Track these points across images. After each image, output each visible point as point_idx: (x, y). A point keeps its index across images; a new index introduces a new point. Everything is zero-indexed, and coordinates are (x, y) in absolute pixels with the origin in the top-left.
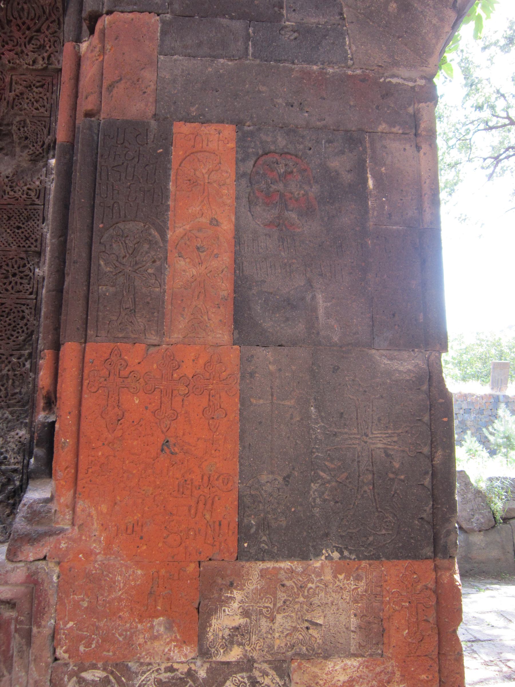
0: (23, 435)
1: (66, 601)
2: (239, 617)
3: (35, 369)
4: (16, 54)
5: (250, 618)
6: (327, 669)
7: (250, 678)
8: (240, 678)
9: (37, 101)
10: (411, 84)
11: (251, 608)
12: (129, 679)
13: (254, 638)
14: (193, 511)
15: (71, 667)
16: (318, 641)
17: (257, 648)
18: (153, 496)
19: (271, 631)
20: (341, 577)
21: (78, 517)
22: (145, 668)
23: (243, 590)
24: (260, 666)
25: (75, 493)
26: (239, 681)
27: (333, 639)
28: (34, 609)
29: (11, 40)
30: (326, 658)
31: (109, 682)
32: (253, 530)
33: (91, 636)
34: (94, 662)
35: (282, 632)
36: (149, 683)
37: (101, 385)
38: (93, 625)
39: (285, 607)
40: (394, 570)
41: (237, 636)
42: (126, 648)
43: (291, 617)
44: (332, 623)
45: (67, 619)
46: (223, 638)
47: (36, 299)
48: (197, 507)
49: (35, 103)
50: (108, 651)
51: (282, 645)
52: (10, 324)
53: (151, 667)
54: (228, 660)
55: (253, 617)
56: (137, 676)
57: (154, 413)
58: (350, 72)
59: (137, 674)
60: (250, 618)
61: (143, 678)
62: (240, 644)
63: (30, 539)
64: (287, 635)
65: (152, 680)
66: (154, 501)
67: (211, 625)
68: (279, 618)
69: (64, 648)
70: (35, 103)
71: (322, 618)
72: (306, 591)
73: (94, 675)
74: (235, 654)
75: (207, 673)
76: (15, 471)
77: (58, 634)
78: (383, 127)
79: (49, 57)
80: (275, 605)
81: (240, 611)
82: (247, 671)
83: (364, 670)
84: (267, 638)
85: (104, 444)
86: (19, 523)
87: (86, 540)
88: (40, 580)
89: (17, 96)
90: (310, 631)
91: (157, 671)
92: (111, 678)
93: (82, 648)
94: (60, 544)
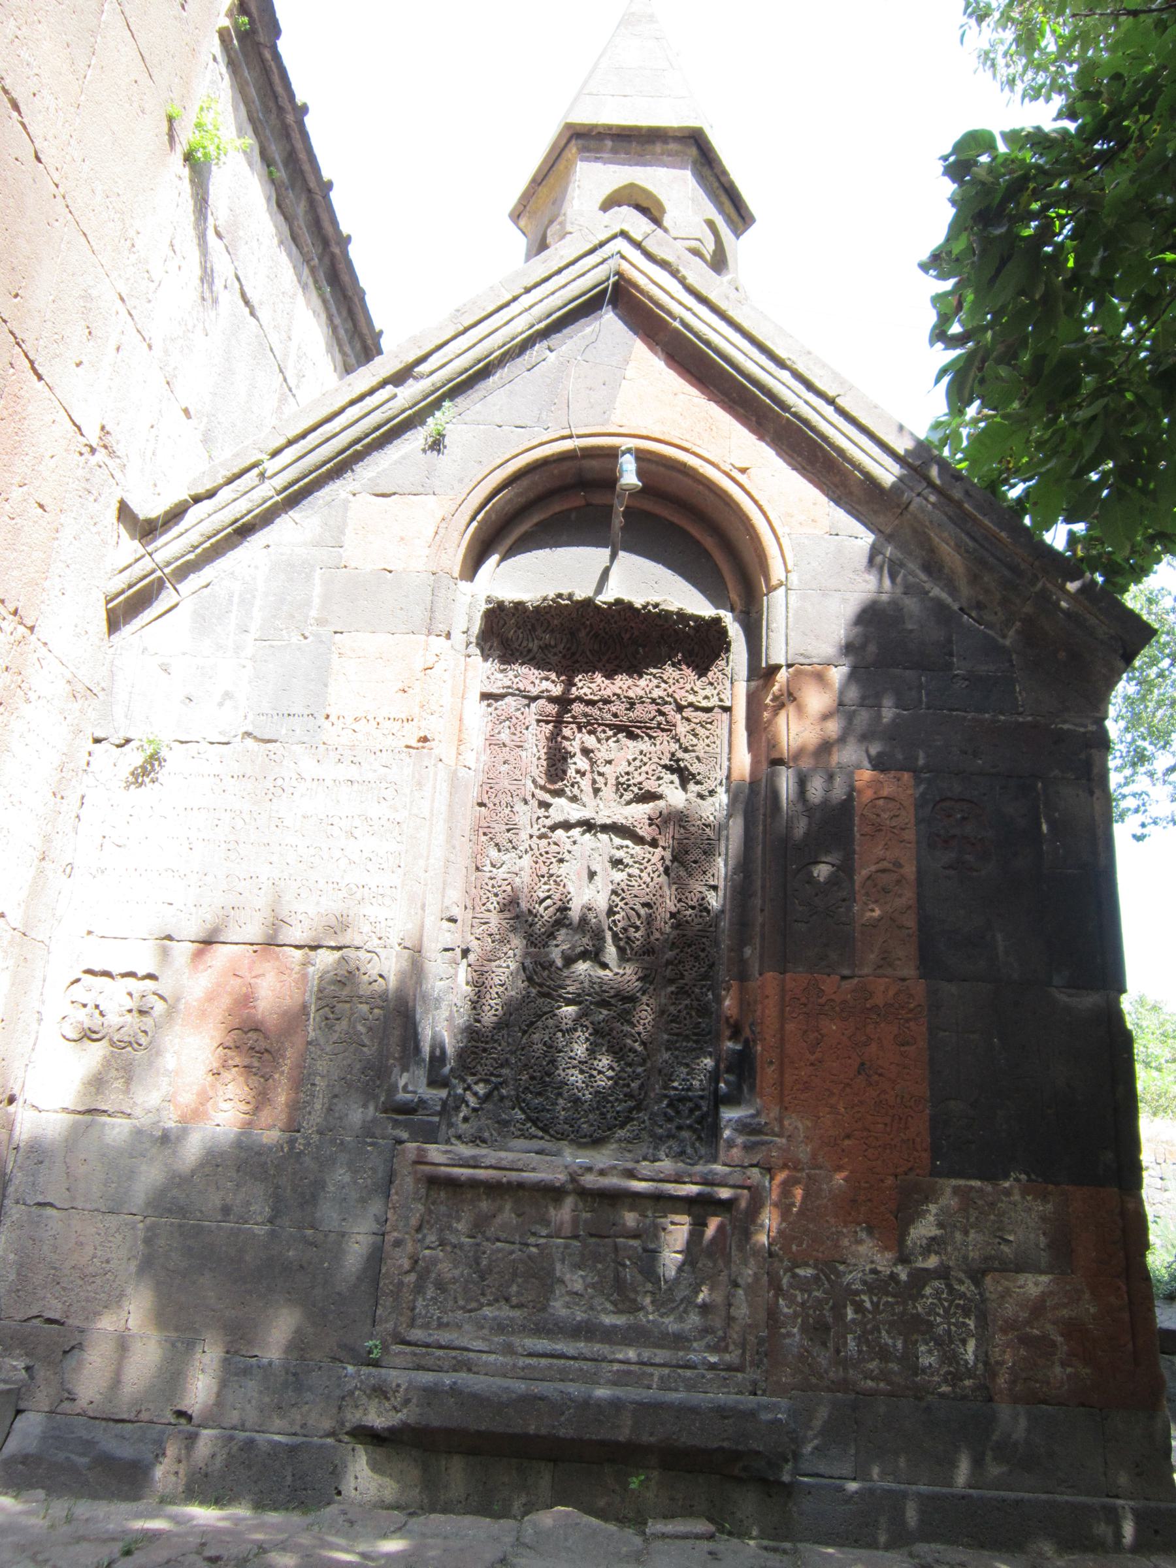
3: (719, 1000)
10: (1082, 730)
13: (949, 1249)
14: (888, 1129)
20: (1029, 1198)
30: (1017, 1272)
31: (820, 1279)
46: (921, 1246)
55: (948, 1230)
57: (849, 1038)
58: (1021, 720)
59: (844, 1273)
62: (937, 1253)
68: (972, 1234)
74: (932, 1262)
76: (702, 1097)
78: (1056, 772)
93: (794, 1248)
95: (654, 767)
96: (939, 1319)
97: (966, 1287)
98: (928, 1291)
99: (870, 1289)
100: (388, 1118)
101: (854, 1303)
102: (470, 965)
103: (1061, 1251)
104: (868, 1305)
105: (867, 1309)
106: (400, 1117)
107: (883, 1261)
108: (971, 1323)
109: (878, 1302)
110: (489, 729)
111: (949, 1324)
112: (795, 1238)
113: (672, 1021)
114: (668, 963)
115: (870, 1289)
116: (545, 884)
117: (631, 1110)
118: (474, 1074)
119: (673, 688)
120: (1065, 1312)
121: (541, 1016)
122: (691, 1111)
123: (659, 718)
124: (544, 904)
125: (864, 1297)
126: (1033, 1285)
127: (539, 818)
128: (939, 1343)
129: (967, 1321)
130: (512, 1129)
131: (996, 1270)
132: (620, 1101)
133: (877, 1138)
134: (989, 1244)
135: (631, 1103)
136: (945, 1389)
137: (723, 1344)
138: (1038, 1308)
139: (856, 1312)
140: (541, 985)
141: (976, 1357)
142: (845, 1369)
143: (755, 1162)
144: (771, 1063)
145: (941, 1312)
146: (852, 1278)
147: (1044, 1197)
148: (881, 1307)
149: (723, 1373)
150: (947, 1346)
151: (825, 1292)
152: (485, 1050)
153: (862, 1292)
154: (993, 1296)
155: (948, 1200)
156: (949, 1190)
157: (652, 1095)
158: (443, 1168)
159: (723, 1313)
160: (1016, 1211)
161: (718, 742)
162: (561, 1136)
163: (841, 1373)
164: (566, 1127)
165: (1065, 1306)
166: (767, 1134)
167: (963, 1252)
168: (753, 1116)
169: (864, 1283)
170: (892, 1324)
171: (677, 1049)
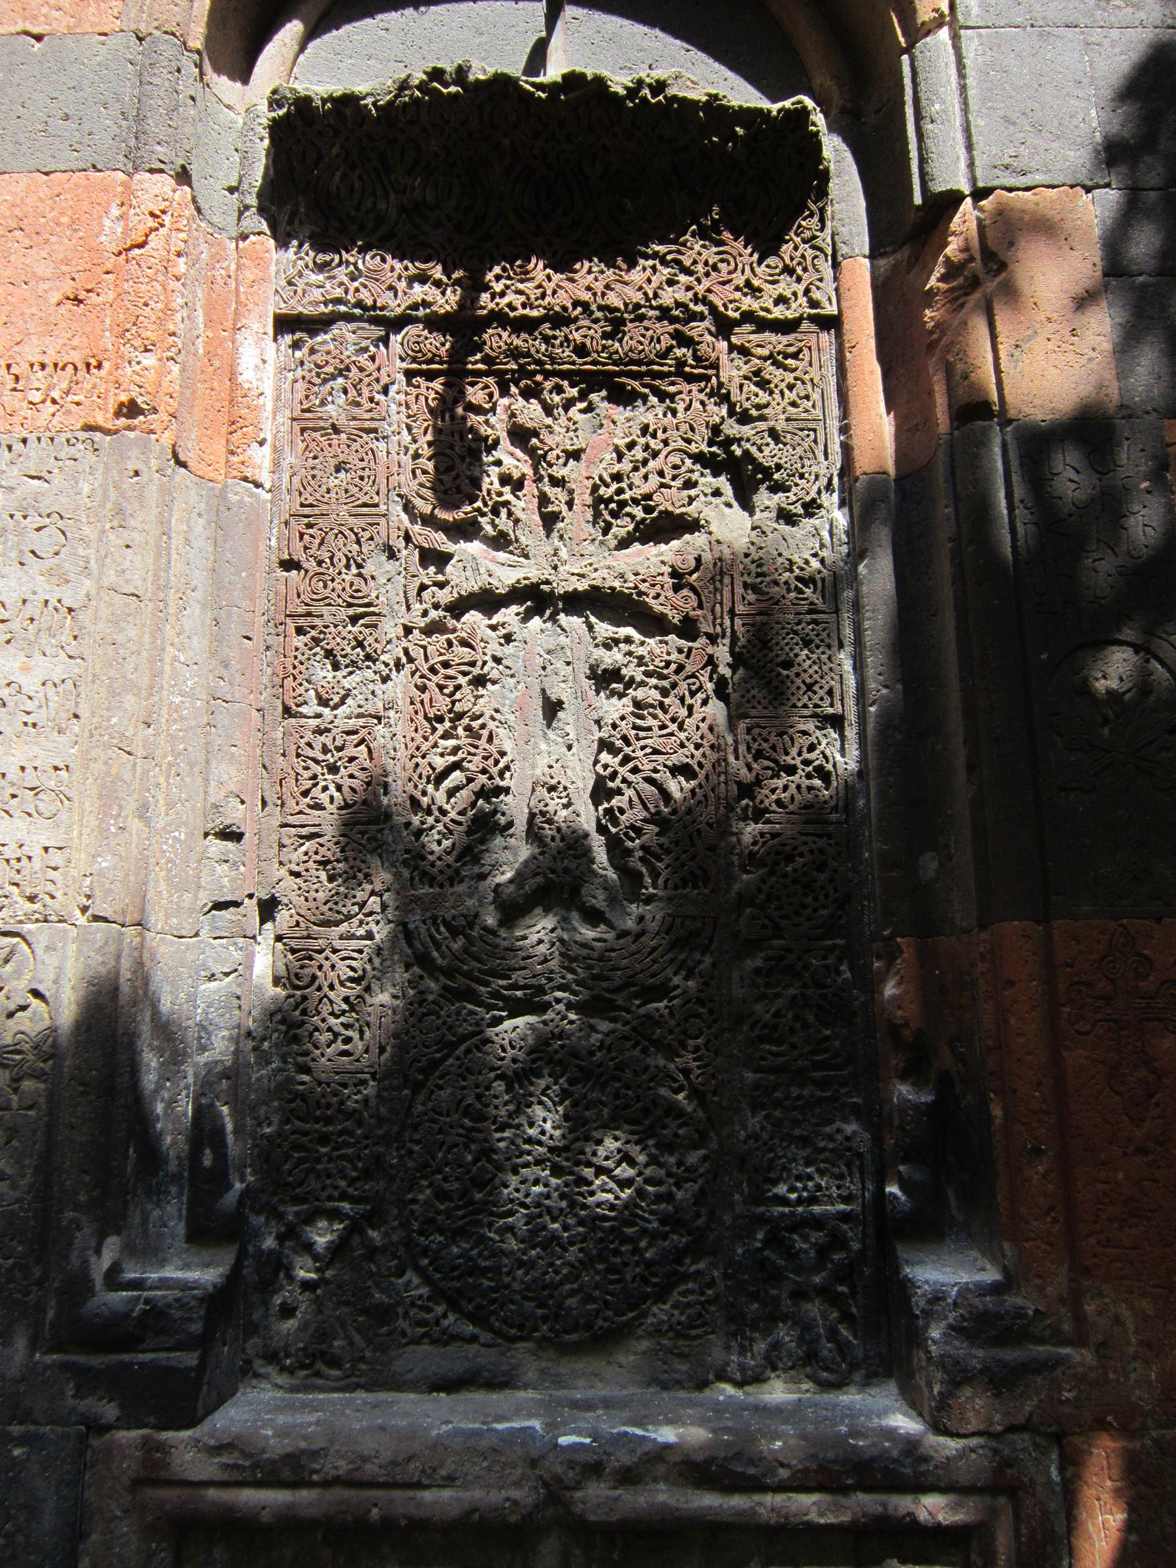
0: (854, 1132)
4: (737, 289)
9: (791, 387)
29: (722, 261)
37: (1099, 1016)
47: (846, 822)
49: (786, 392)
52: (795, 882)
70: (786, 392)
76: (845, 1217)
79: (807, 292)
85: (1125, 1154)
87: (1118, 1381)
89: (746, 378)
95: (675, 459)
100: (65, 1366)
102: (279, 938)
106: (97, 1361)
110: (300, 395)
113: (762, 1039)
114: (744, 900)
116: (446, 736)
117: (678, 1256)
118: (297, 1200)
119: (706, 283)
121: (453, 1046)
122: (823, 1252)
123: (679, 352)
124: (447, 783)
127: (423, 587)
130: (402, 1323)
132: (654, 1236)
135: (679, 1240)
140: (449, 972)
143: (1021, 1419)
144: (1037, 1152)
152: (324, 1139)
157: (728, 1218)
158: (212, 1493)
161: (816, 396)
162: (522, 1329)
164: (529, 1305)
166: (1042, 1341)
168: (995, 1289)
171: (777, 1104)
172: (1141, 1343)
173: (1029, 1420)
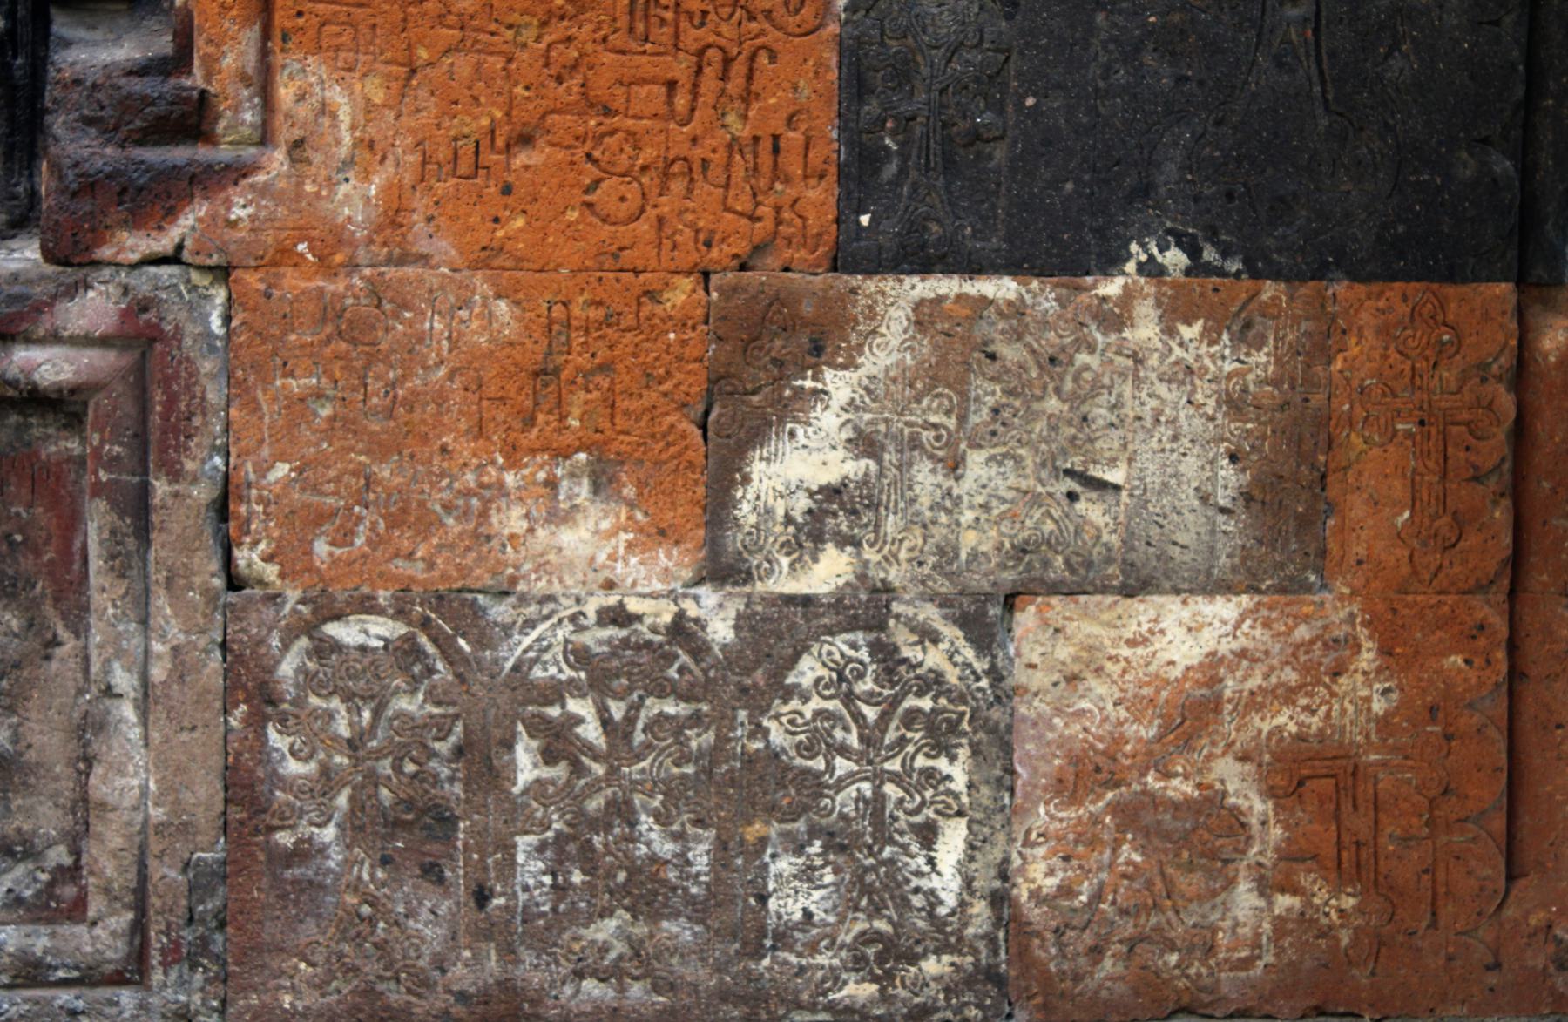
1: (260, 394)
2: (841, 453)
5: (879, 461)
6: (1134, 628)
7: (876, 648)
8: (845, 648)
11: (882, 428)
12: (482, 642)
13: (891, 524)
14: (681, 101)
15: (288, 607)
16: (1105, 538)
17: (903, 555)
18: (543, 46)
19: (949, 502)
20: (1189, 332)
21: (288, 116)
22: (532, 610)
23: (857, 367)
24: (910, 611)
25: (266, 35)
26: (842, 655)
27: (1155, 532)
28: (156, 420)
31: (417, 653)
32: (891, 169)
33: (349, 508)
34: (366, 590)
35: (986, 507)
36: (547, 657)
38: (355, 474)
39: (998, 426)
40: (1369, 314)
41: (835, 515)
42: (468, 549)
43: (1018, 460)
44: (1154, 480)
45: (266, 452)
46: (789, 520)
48: (695, 85)
50: (410, 556)
51: (983, 548)
53: (552, 606)
54: (806, 591)
56: (509, 636)
59: (507, 629)
60: (879, 461)
61: (527, 641)
62: (843, 541)
63: (124, 190)
64: (1002, 516)
65: (559, 649)
66: (547, 65)
67: (746, 480)
68: (976, 463)
69: (262, 546)
71: (1123, 465)
72: (1069, 378)
73: (366, 632)
74: (828, 572)
75: (737, 628)
77: (240, 499)
80: (962, 419)
81: (844, 435)
82: (867, 628)
83: (1258, 632)
84: (934, 522)
86: (73, 144)
88: (168, 328)
90: (1080, 506)
91: (573, 619)
92: (423, 639)
93: (321, 548)
94: (228, 209)
96: (842, 765)
97: (947, 655)
98: (808, 671)
99: (599, 675)
101: (538, 727)
103: (1288, 518)
104: (591, 731)
105: (589, 749)
107: (655, 585)
108: (958, 772)
109: (630, 720)
111: (879, 778)
112: (321, 517)
115: (599, 675)
120: (1285, 720)
125: (580, 707)
126: (1188, 632)
128: (839, 842)
129: (942, 764)
131: (1054, 589)
133: (633, 138)
134: (1036, 500)
136: (859, 990)
137: (69, 891)
138: (1192, 712)
139: (549, 756)
141: (968, 883)
142: (508, 952)
145: (853, 740)
146: (538, 645)
147: (1246, 335)
148: (639, 737)
149: (65, 997)
150: (865, 854)
151: (433, 697)
153: (573, 687)
154: (1038, 679)
155: (889, 346)
156: (896, 322)
159: (67, 786)
160: (1138, 382)
163: (493, 963)
165: (1288, 695)
167: (939, 533)
169: (579, 656)
170: (673, 792)
172: (357, 143)
173: (180, 247)
